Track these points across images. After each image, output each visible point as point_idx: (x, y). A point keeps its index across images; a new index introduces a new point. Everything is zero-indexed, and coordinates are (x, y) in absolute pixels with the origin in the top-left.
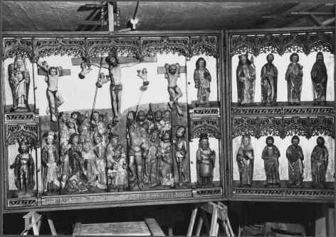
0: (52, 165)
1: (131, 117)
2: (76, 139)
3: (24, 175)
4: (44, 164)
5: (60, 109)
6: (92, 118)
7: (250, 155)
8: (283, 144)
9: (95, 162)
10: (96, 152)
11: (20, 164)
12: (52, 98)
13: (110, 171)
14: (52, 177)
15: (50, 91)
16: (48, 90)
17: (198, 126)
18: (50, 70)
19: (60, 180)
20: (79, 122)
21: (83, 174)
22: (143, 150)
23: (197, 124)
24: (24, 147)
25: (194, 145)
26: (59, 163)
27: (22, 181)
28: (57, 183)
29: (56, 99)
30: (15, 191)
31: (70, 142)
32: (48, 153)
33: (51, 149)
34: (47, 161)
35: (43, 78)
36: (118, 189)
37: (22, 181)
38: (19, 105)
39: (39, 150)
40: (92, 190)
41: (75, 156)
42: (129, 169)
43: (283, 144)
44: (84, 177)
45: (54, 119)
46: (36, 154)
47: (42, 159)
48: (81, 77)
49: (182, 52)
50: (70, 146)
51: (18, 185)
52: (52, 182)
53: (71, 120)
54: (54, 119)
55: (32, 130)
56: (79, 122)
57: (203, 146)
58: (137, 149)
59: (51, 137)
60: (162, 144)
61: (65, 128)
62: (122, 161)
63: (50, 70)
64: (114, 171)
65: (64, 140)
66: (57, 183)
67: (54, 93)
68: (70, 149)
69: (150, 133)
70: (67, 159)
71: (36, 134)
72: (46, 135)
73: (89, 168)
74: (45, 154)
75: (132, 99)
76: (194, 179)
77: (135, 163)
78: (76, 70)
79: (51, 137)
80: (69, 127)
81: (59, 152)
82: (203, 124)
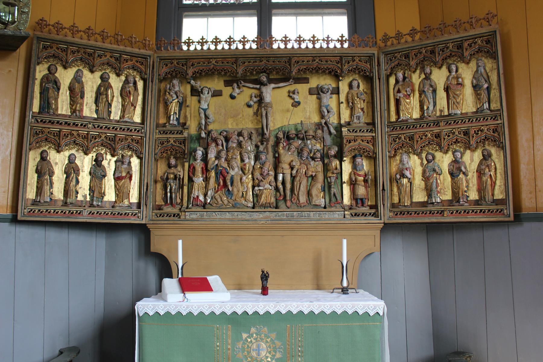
0: (199, 180)
1: (281, 135)
2: (223, 154)
3: (171, 189)
4: (191, 180)
5: (210, 127)
6: (240, 134)
7: (407, 173)
8: (444, 161)
9: (241, 179)
10: (243, 170)
11: (167, 178)
12: (203, 116)
13: (256, 188)
15: (202, 109)
16: (199, 107)
17: (351, 144)
18: (202, 89)
19: (205, 195)
20: (227, 139)
21: (229, 190)
22: (292, 168)
23: (350, 142)
24: (173, 161)
25: (347, 167)
26: (206, 180)
27: (169, 194)
28: (201, 198)
29: (207, 117)
30: (162, 205)
31: (218, 157)
32: (194, 168)
33: (199, 165)
34: (194, 175)
35: (195, 98)
36: (264, 206)
37: (169, 194)
38: (171, 122)
39: (187, 165)
41: (221, 174)
42: (277, 189)
43: (444, 161)
44: (229, 193)
45: (203, 135)
46: (183, 172)
47: (189, 174)
48: (232, 97)
50: (216, 162)
51: (165, 200)
52: (198, 197)
53: (219, 137)
54: (203, 135)
55: (181, 144)
56: (227, 139)
57: (355, 167)
58: (286, 166)
59: (199, 153)
60: (312, 163)
61: (214, 145)
63: (202, 89)
64: (261, 188)
65: (212, 155)
66: (201, 198)
67: (205, 110)
68: (217, 165)
69: (300, 153)
70: (213, 174)
71: (184, 148)
72: (195, 151)
73: (235, 184)
76: (347, 200)
77: (284, 183)
78: (227, 91)
79: (199, 153)
80: (217, 145)
81: (206, 170)
82: (357, 143)
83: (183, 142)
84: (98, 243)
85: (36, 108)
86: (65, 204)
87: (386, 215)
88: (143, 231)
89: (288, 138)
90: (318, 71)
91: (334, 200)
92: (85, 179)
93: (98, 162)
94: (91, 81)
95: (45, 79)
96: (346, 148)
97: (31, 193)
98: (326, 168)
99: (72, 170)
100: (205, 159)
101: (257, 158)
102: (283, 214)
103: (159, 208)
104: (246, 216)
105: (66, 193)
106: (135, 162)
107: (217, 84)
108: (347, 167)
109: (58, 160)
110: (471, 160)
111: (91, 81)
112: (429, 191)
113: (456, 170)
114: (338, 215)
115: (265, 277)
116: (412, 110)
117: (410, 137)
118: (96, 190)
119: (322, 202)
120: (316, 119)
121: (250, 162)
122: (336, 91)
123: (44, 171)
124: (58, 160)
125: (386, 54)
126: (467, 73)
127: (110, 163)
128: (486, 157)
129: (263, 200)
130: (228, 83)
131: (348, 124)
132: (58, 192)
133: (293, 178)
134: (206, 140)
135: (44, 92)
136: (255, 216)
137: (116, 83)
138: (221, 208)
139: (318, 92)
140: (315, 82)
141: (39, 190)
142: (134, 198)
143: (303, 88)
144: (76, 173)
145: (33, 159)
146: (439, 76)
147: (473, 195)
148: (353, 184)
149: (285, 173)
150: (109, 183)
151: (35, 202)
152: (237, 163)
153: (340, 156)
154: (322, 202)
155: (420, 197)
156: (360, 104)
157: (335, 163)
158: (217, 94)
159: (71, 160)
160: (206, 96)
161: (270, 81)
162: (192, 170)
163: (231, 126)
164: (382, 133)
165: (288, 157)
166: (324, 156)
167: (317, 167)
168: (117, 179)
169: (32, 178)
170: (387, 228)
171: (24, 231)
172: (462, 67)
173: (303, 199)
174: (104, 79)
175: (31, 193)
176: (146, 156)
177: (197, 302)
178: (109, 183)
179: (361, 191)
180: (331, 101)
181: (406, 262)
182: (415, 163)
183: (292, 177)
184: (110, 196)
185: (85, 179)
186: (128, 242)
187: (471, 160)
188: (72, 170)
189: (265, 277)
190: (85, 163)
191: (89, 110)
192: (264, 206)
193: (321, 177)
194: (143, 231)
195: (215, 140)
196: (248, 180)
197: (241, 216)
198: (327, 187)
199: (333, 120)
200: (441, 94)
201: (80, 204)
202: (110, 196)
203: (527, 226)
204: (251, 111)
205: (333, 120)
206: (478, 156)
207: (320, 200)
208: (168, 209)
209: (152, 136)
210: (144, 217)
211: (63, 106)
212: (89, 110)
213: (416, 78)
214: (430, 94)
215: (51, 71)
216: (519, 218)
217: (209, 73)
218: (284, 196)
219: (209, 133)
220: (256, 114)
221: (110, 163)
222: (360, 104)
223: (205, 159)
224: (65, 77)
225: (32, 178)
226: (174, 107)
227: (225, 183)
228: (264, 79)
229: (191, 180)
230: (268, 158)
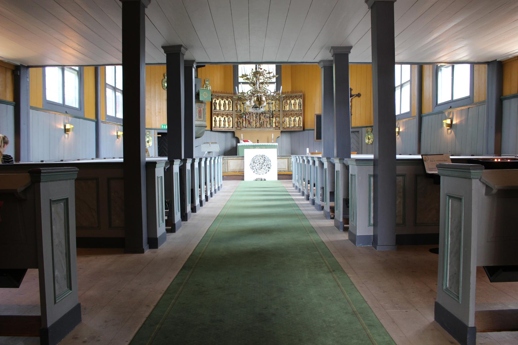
0: (244, 122)
8: (293, 119)
14: (244, 125)
33: (244, 119)
41: (249, 121)
43: (293, 119)
65: (247, 117)
74: (243, 120)
81: (246, 120)
87: (282, 129)
88: (233, 133)
91: (271, 126)
92: (222, 123)
93: (224, 118)
94: (222, 102)
97: (213, 125)
99: (220, 121)
100: (245, 118)
102: (261, 129)
110: (297, 119)
111: (222, 102)
112: (289, 125)
113: (294, 120)
114: (272, 129)
116: (287, 108)
117: (287, 114)
121: (255, 118)
122: (272, 103)
123: (215, 121)
126: (297, 101)
127: (226, 119)
128: (300, 118)
132: (218, 125)
134: (245, 114)
137: (227, 102)
141: (215, 125)
142: (231, 126)
144: (221, 122)
146: (293, 102)
147: (297, 126)
148: (275, 123)
150: (227, 123)
152: (252, 119)
153: (273, 117)
155: (288, 126)
156: (277, 106)
162: (243, 120)
164: (281, 113)
165: (262, 117)
167: (268, 119)
169: (213, 122)
170: (282, 132)
171: (212, 133)
174: (225, 101)
178: (227, 123)
179: (277, 124)
180: (271, 106)
181: (286, 139)
182: (287, 119)
183: (263, 120)
184: (227, 126)
185: (222, 123)
186: (229, 135)
187: (297, 119)
188: (220, 121)
190: (222, 119)
191: (222, 108)
194: (233, 133)
196: (254, 122)
198: (270, 124)
199: (271, 110)
200: (293, 106)
202: (227, 126)
203: (306, 132)
205: (271, 110)
206: (298, 118)
207: (269, 126)
209: (235, 113)
210: (234, 130)
211: (218, 108)
212: (222, 108)
213: (288, 102)
216: (304, 130)
218: (261, 125)
221: (226, 119)
222: (277, 106)
223: (245, 118)
224: (218, 102)
226: (239, 107)
227: (250, 123)
230: (258, 118)
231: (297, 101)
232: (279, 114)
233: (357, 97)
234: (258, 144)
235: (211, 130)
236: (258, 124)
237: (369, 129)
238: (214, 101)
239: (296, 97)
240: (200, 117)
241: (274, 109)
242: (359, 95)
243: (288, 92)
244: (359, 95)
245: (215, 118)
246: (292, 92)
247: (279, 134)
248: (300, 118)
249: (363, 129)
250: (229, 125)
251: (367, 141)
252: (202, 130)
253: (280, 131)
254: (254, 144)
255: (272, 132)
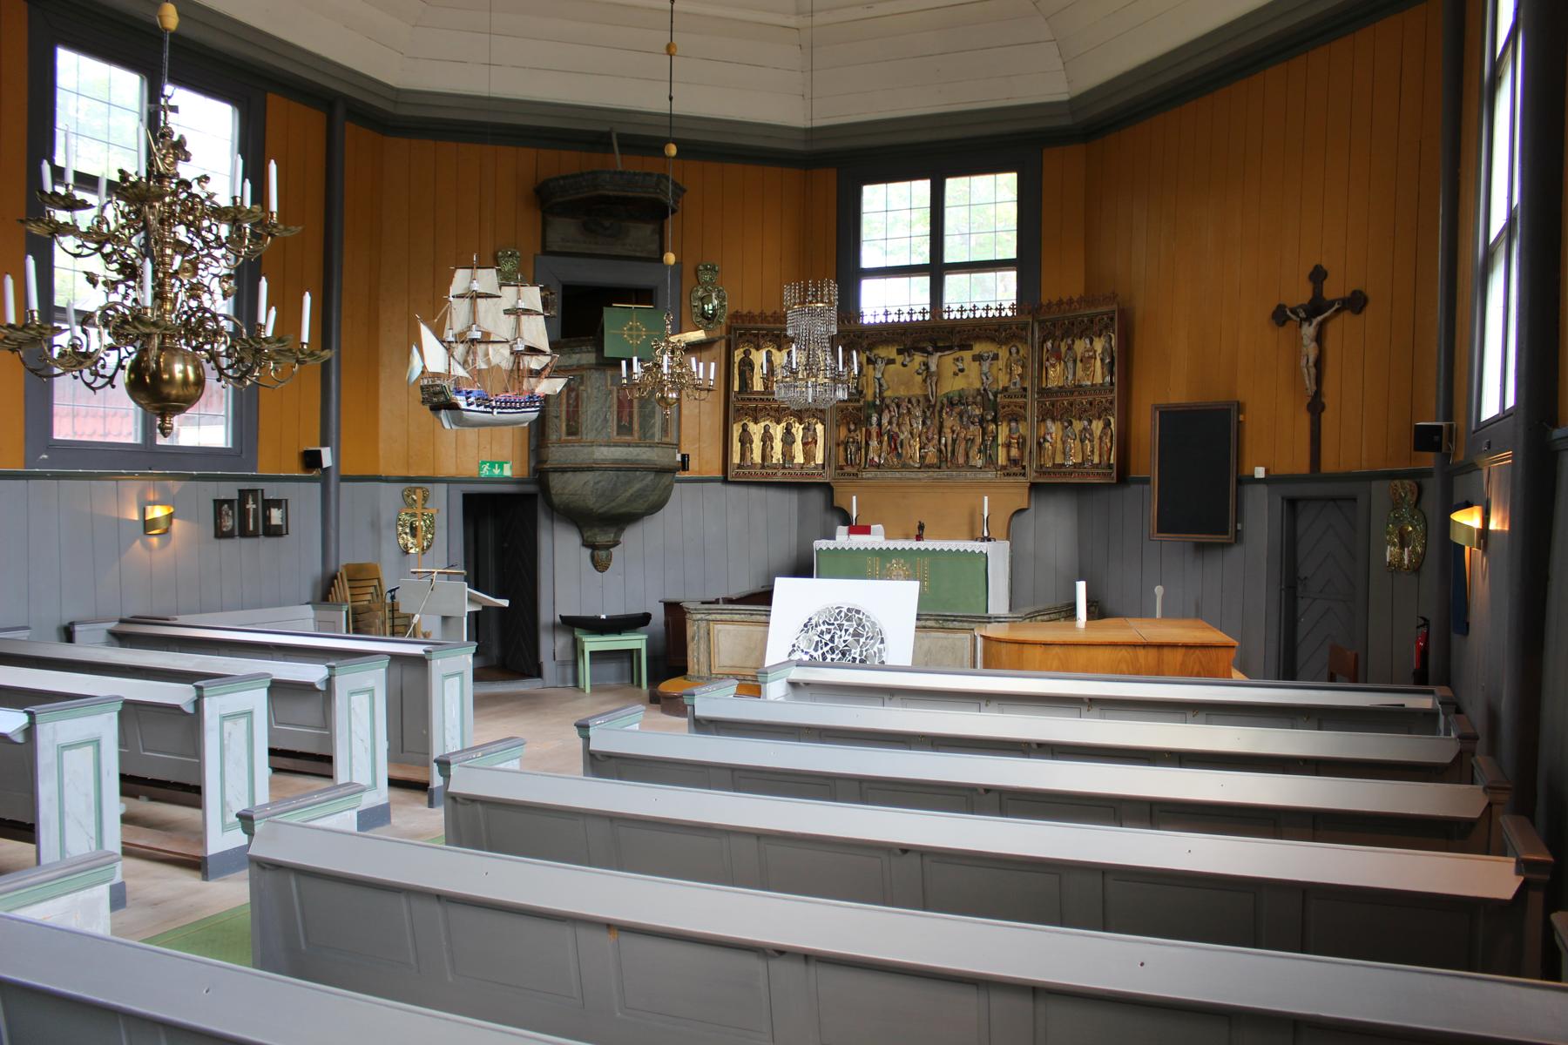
0: (874, 443)
6: (910, 401)
26: (880, 442)
31: (890, 423)
33: (874, 429)
36: (930, 466)
40: (905, 466)
41: (893, 438)
42: (940, 451)
44: (899, 455)
46: (860, 436)
49: (992, 340)
56: (898, 406)
59: (874, 419)
62: (935, 442)
65: (885, 421)
69: (961, 415)
75: (952, 385)
76: (1002, 459)
78: (899, 359)
79: (874, 419)
81: (880, 435)
83: (859, 409)
84: (790, 499)
85: (736, 388)
86: (763, 467)
87: (1032, 476)
88: (827, 488)
89: (952, 404)
90: (978, 338)
91: (991, 461)
92: (778, 445)
93: (788, 431)
95: (742, 362)
96: (1001, 412)
97: (736, 459)
98: (984, 433)
99: (767, 438)
100: (879, 424)
101: (924, 423)
103: (841, 468)
104: (913, 475)
105: (764, 457)
106: (820, 428)
107: (892, 352)
108: (1003, 433)
109: (756, 430)
114: (991, 475)
115: (921, 527)
118: (787, 454)
119: (979, 463)
120: (977, 385)
123: (746, 439)
124: (756, 430)
125: (1040, 323)
127: (798, 430)
128: (1108, 424)
129: (927, 461)
130: (900, 352)
131: (1005, 389)
132: (757, 457)
133: (954, 441)
135: (741, 374)
136: (921, 475)
138: (892, 468)
139: (978, 358)
140: (978, 348)
142: (819, 461)
143: (967, 355)
145: (736, 431)
147: (1096, 460)
149: (948, 437)
150: (798, 449)
151: (739, 466)
154: (979, 463)
157: (992, 427)
158: (891, 361)
159: (766, 429)
160: (880, 365)
161: (937, 349)
162: (868, 434)
163: (902, 392)
165: (950, 421)
166: (982, 420)
167: (975, 430)
168: (805, 444)
169: (737, 446)
170: (1034, 487)
172: (1096, 340)
173: (961, 460)
175: (736, 459)
176: (828, 422)
177: (859, 541)
178: (798, 449)
179: (1014, 452)
186: (816, 499)
188: (767, 438)
189: (921, 527)
190: (778, 431)
192: (930, 466)
193: (979, 440)
195: (888, 407)
197: (908, 475)
201: (774, 467)
203: (1134, 487)
204: (919, 378)
208: (848, 469)
211: (758, 385)
214: (1070, 365)
215: (747, 353)
217: (886, 342)
218: (945, 459)
219: (883, 400)
220: (925, 381)
221: (798, 430)
223: (879, 424)
225: (737, 446)
227: (895, 443)
228: (930, 349)
229: (867, 444)
231: (1099, 345)
232: (1024, 407)
233: (1346, 316)
234: (922, 545)
235: (725, 481)
236: (931, 450)
237: (1405, 488)
238: (738, 355)
239: (1087, 329)
240: (625, 429)
241: (1003, 380)
242: (1356, 303)
243: (1071, 301)
244: (1356, 303)
245: (745, 429)
246: (1088, 299)
247: (1019, 498)
248: (1108, 424)
249: (1374, 484)
250: (809, 456)
251: (1390, 552)
252: (637, 486)
253: (1024, 482)
254: (900, 544)
255: (985, 486)
